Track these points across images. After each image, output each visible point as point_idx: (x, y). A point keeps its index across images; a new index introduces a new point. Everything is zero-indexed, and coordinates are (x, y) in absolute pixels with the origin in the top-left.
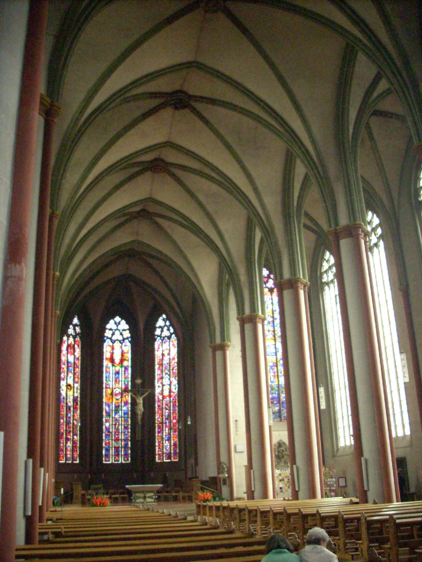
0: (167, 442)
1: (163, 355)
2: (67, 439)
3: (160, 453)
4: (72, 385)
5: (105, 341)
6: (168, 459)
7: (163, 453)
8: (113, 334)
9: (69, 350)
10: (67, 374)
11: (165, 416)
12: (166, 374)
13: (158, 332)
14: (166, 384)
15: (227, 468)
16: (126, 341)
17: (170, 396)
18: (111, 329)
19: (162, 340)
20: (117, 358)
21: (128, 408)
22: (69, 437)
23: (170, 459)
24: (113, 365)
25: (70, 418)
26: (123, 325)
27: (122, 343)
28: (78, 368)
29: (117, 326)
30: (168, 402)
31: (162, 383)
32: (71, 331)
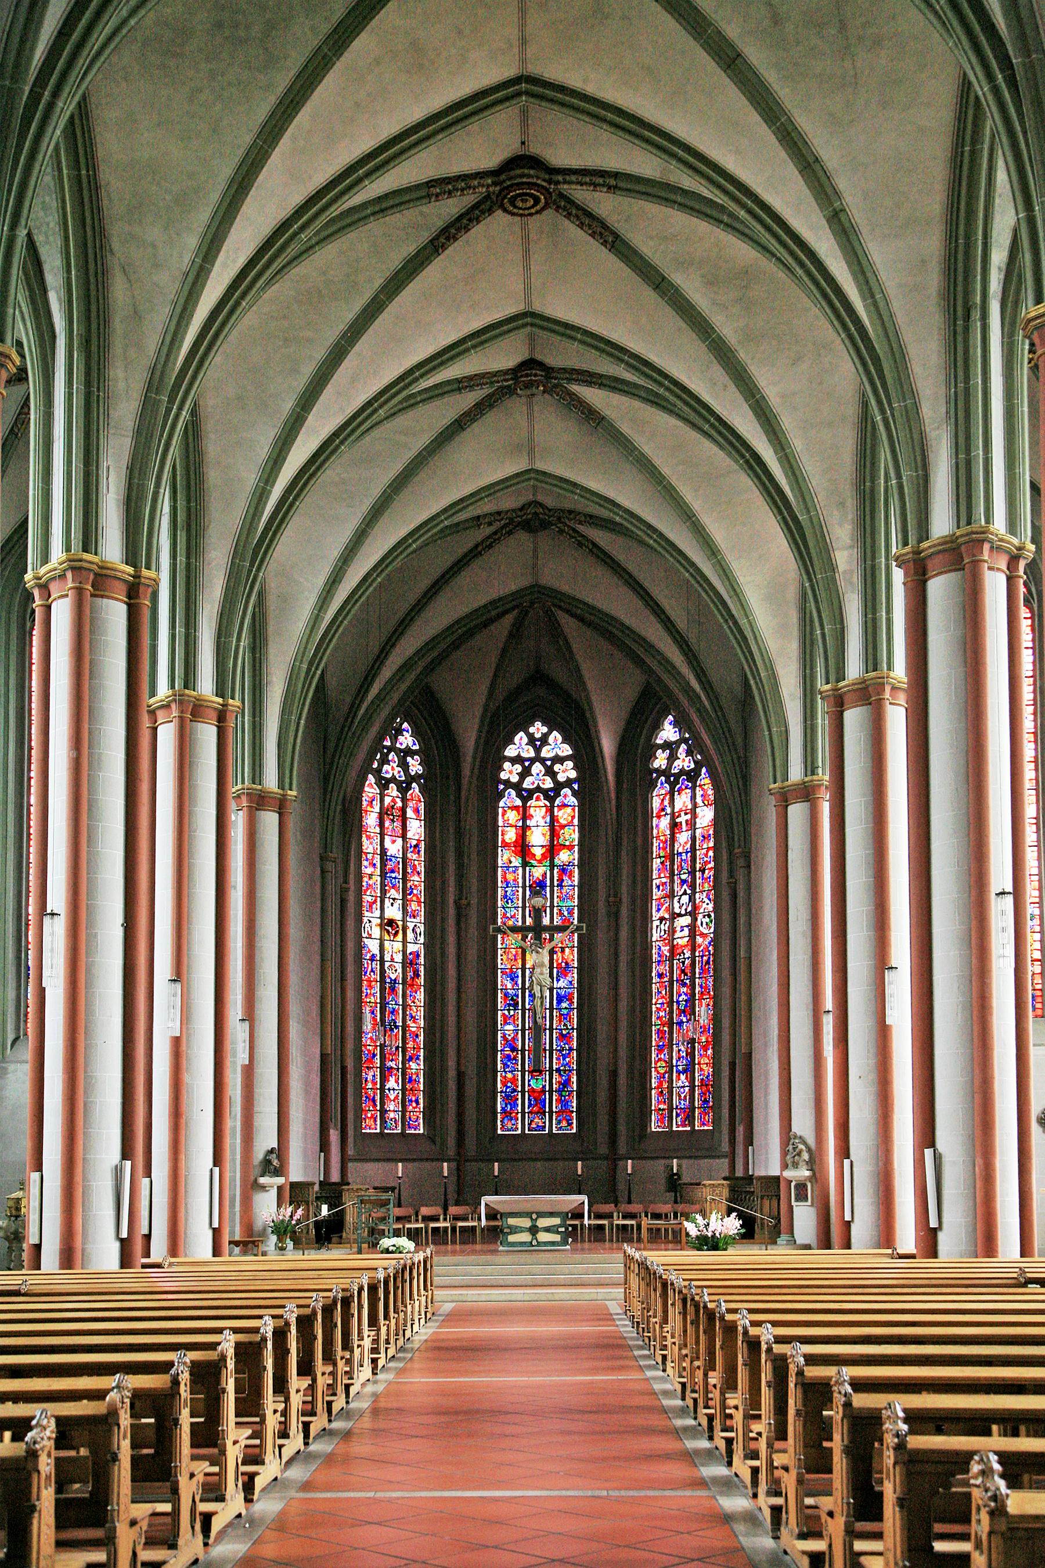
1: (674, 826)
2: (386, 1073)
3: (662, 1106)
4: (400, 923)
5: (501, 795)
8: (526, 773)
9: (387, 824)
10: (384, 892)
13: (660, 760)
14: (683, 912)
16: (566, 791)
18: (517, 760)
19: (673, 785)
22: (392, 1064)
24: (525, 864)
25: (393, 1012)
26: (557, 746)
27: (552, 800)
29: (538, 750)
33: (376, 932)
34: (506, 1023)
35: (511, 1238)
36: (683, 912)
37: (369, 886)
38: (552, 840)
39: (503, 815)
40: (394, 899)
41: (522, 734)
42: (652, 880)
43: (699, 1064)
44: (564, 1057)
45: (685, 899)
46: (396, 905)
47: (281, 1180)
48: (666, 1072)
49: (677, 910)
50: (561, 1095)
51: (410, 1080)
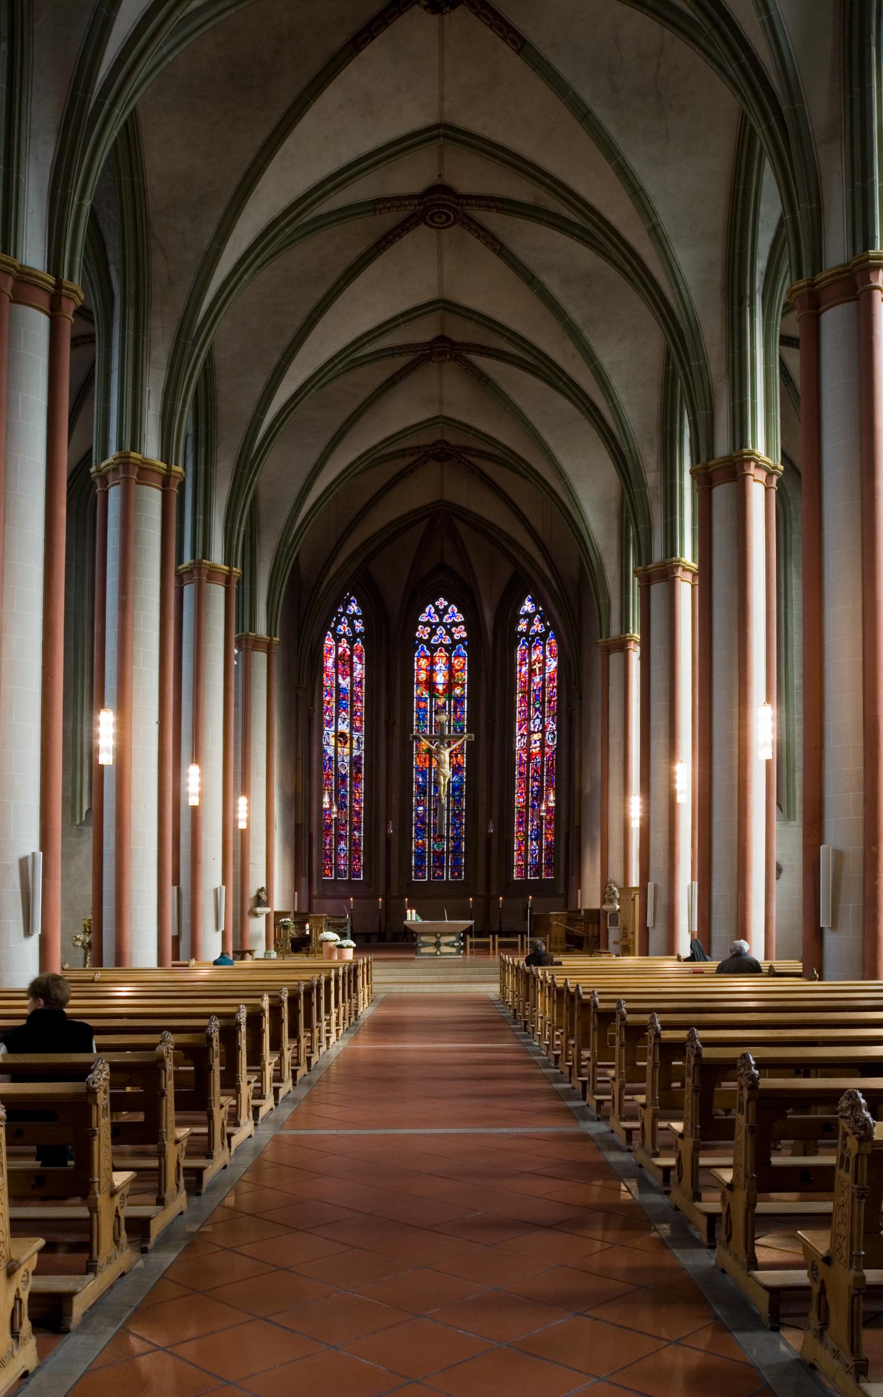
0: (534, 843)
1: (531, 672)
2: (339, 838)
3: (520, 863)
4: (348, 735)
6: (534, 876)
7: (526, 864)
8: (433, 633)
10: (338, 714)
11: (532, 792)
12: (537, 710)
13: (522, 626)
14: (536, 730)
15: (620, 890)
17: (542, 753)
18: (427, 624)
20: (440, 679)
21: (461, 778)
23: (540, 876)
25: (344, 796)
27: (450, 652)
28: (361, 701)
30: (539, 765)
31: (528, 729)
32: (343, 628)
33: (332, 741)
34: (418, 805)
35: (423, 950)
36: (536, 730)
37: (327, 709)
38: (449, 680)
39: (418, 662)
40: (344, 719)
41: (430, 605)
42: (516, 708)
43: (545, 834)
44: (457, 829)
45: (538, 721)
46: (346, 723)
47: (268, 910)
48: (524, 840)
49: (532, 729)
50: (454, 855)
51: (355, 844)
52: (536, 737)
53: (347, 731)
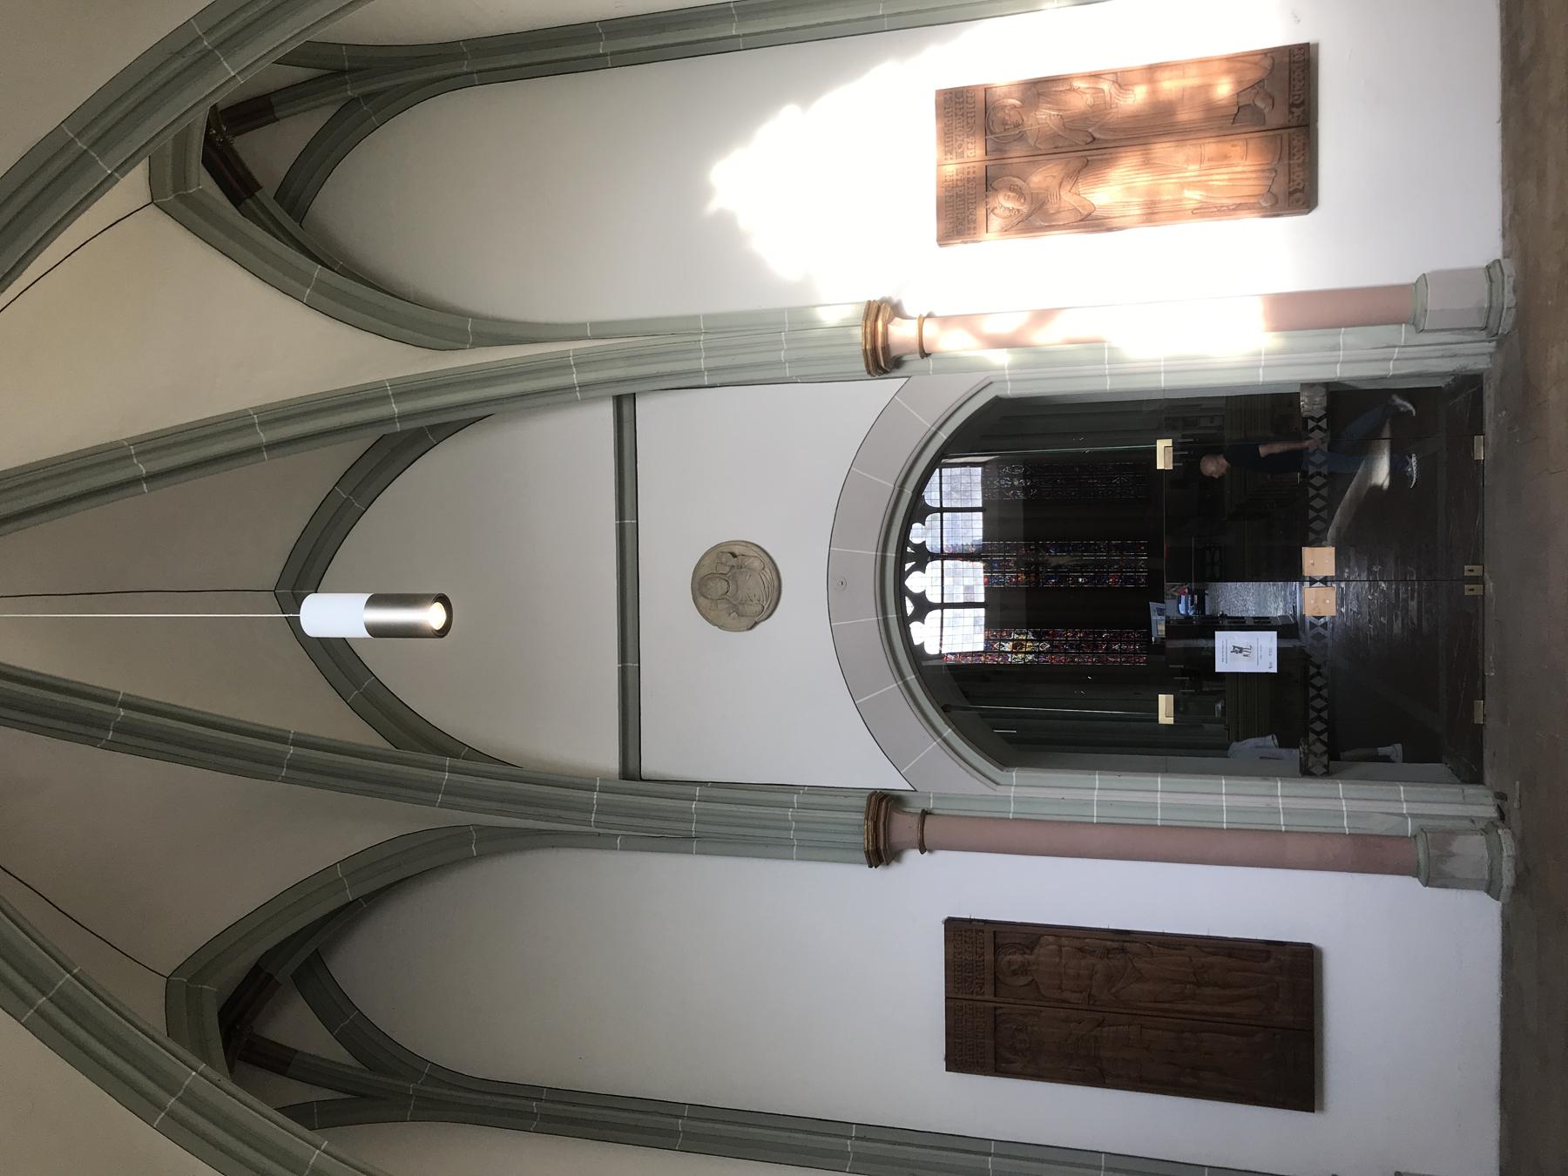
2: (1109, 651)
21: (1052, 545)
40: (1000, 645)
52: (1016, 483)
53: (1011, 643)
